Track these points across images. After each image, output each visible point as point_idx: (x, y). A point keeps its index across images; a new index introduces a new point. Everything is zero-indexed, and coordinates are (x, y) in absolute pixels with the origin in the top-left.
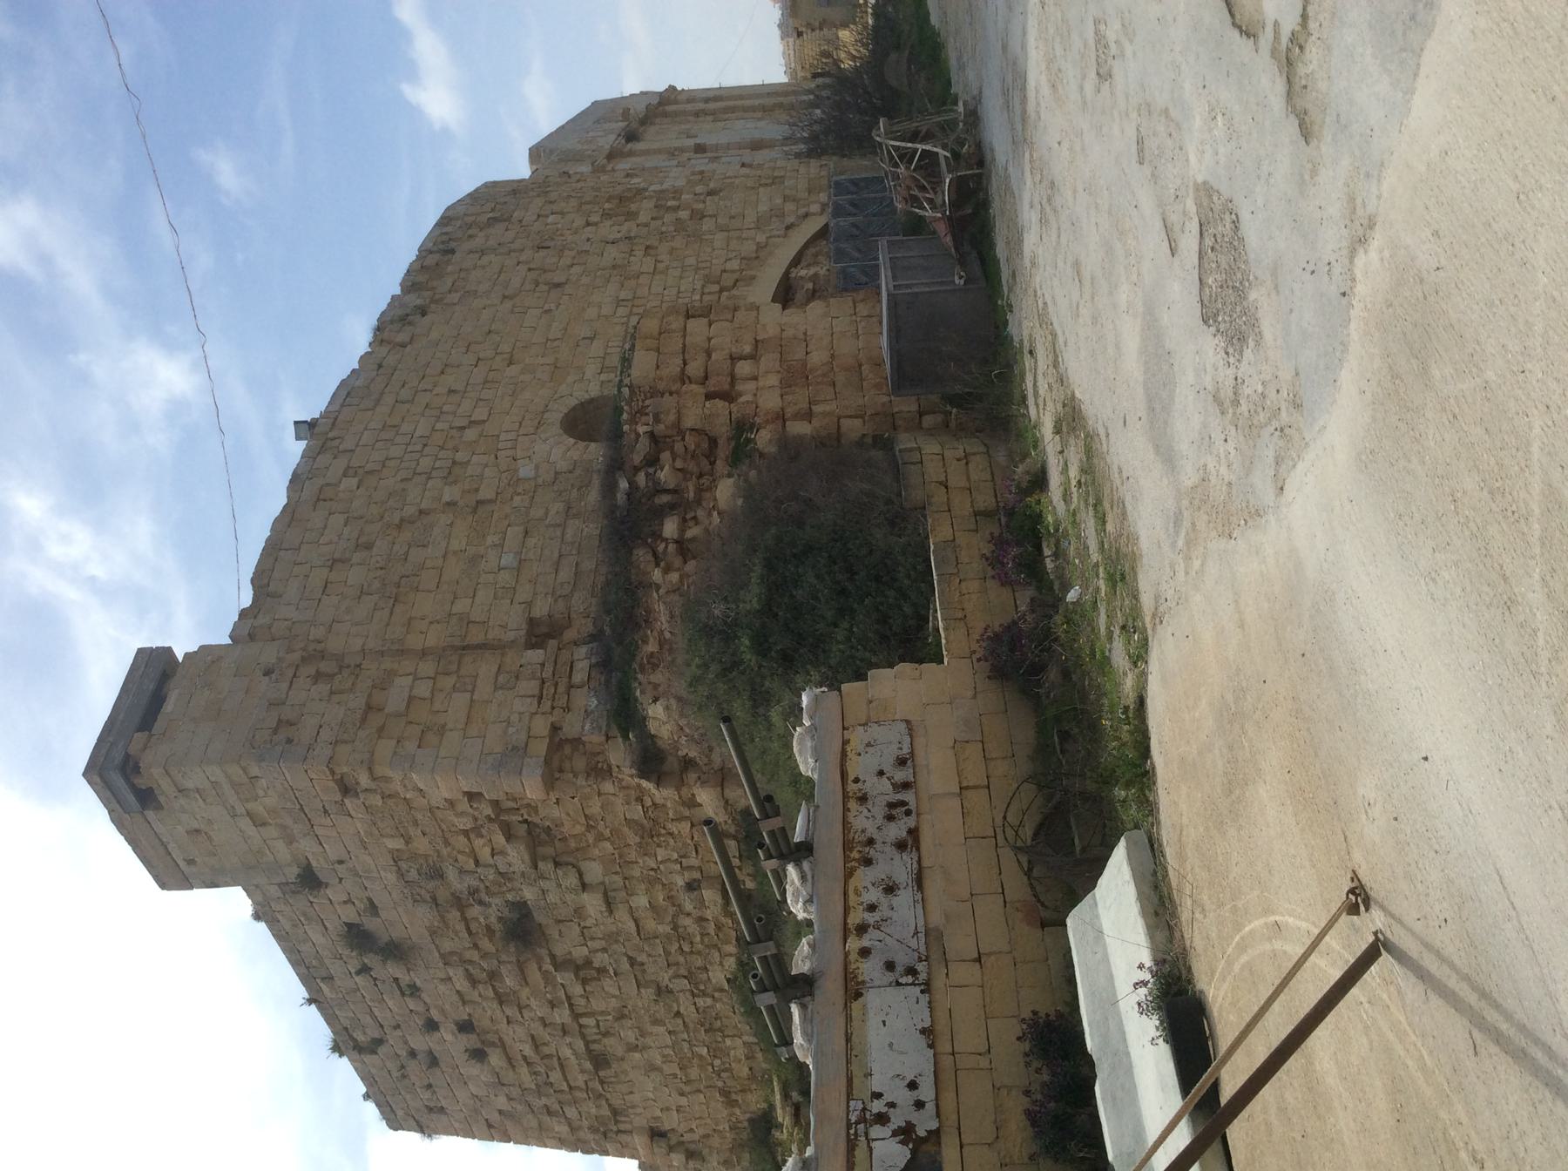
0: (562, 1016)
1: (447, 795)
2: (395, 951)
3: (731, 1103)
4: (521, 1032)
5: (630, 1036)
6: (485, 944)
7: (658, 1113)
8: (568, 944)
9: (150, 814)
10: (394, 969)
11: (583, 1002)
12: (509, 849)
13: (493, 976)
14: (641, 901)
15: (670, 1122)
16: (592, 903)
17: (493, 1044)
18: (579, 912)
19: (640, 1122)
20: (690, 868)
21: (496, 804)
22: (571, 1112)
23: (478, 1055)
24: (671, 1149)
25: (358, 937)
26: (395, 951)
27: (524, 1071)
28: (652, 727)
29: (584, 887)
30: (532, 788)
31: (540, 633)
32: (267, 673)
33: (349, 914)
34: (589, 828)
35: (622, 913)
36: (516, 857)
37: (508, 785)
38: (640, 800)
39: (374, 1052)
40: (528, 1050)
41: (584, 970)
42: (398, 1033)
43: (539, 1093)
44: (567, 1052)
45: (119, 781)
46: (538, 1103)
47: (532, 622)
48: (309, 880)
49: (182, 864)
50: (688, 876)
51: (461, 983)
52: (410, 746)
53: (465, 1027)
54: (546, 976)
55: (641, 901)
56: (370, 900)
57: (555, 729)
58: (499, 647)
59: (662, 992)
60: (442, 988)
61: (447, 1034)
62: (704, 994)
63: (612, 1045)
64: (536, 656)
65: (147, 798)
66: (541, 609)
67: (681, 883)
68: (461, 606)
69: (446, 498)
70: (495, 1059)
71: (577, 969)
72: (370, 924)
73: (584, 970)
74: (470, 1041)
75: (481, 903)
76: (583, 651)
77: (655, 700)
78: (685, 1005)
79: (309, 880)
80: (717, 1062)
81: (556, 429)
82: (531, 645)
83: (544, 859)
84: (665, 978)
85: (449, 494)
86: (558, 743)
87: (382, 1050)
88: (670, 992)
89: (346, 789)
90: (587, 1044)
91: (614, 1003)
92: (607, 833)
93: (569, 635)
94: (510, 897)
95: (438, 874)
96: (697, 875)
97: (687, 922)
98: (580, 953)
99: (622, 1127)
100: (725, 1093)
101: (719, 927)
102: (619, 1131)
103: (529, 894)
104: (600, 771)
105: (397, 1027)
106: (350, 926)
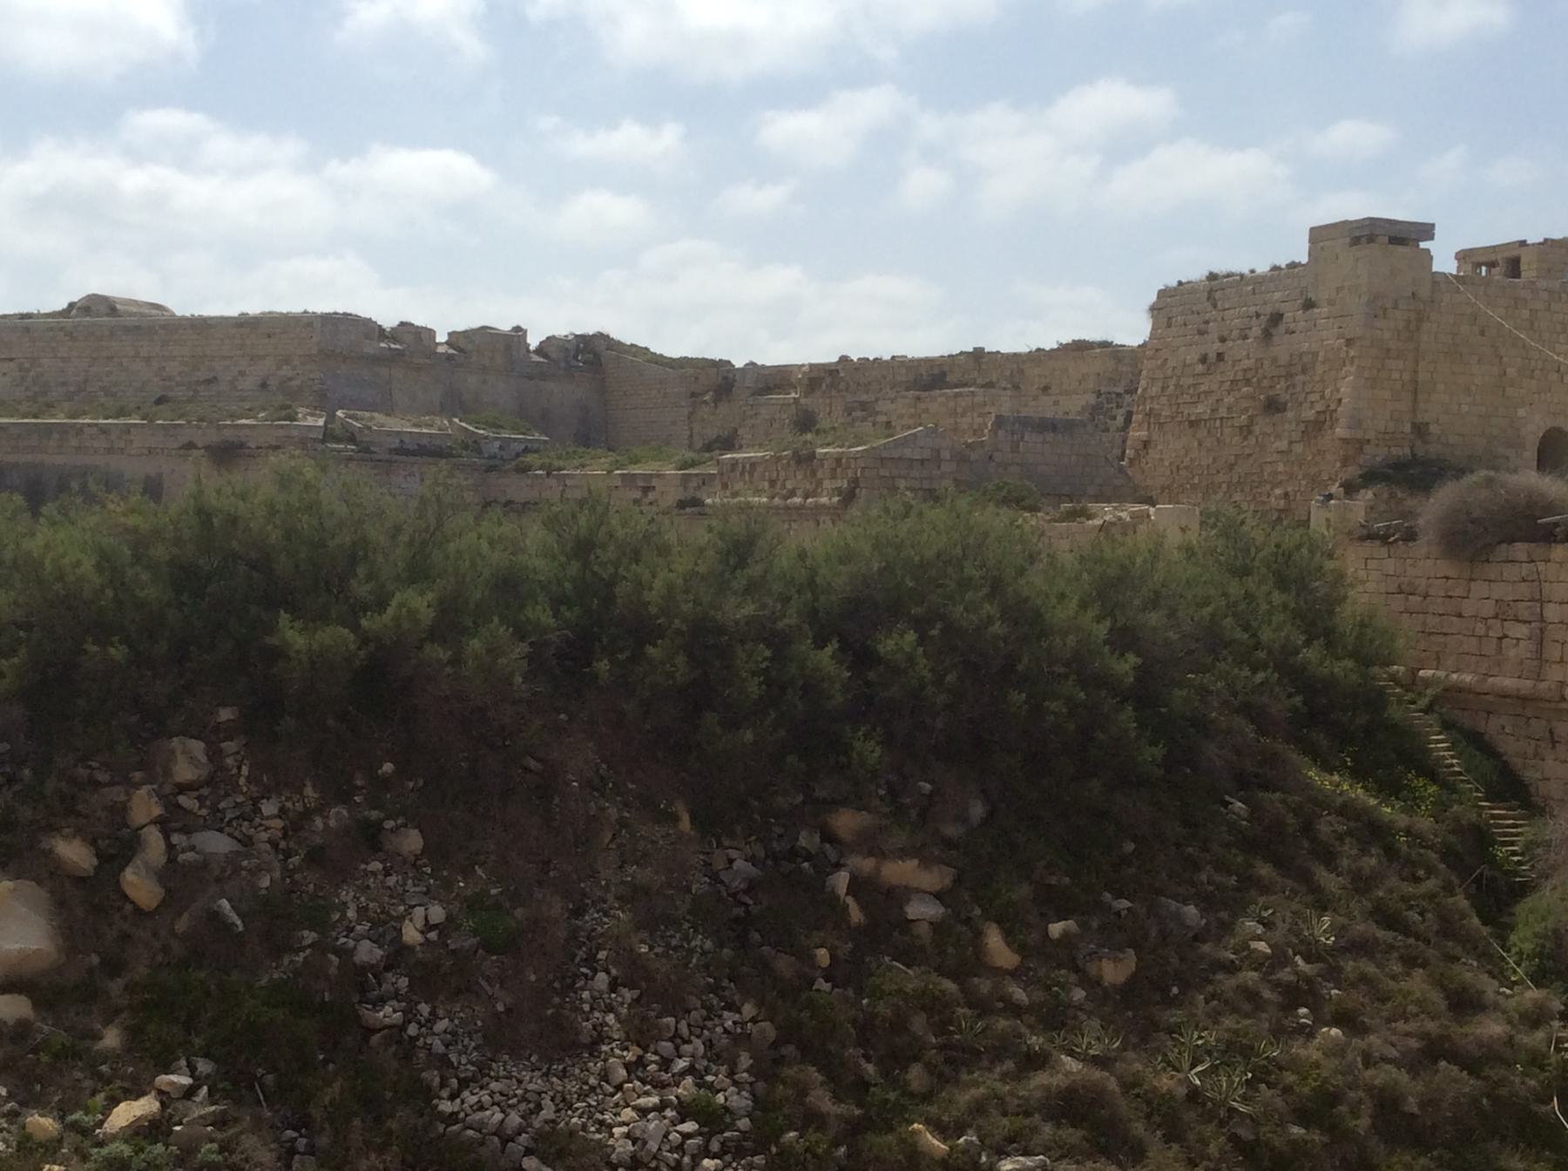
0: (1223, 412)
1: (1342, 390)
2: (1267, 335)
3: (1163, 489)
4: (1215, 387)
5: (1208, 443)
6: (1266, 383)
7: (1159, 447)
8: (1262, 425)
9: (1348, 240)
10: (1256, 331)
11: (1229, 423)
12: (1313, 411)
13: (1248, 382)
14: (1281, 468)
15: (1153, 454)
16: (1283, 445)
17: (1209, 369)
18: (1279, 437)
19: (1155, 437)
20: (1295, 495)
21: (1335, 410)
22: (1164, 400)
23: (1203, 359)
24: (1137, 451)
25: (1277, 318)
26: (1267, 335)
27: (1191, 381)
28: (1362, 491)
29: (1291, 443)
30: (1340, 431)
31: (1420, 430)
32: (1413, 294)
33: (1288, 316)
34: (1319, 451)
35: (1275, 457)
36: (1309, 414)
37: (1343, 421)
38: (1330, 479)
39: (1208, 299)
40: (1203, 388)
41: (1246, 430)
42: (1219, 319)
43: (1176, 386)
44: (1200, 409)
45: (1366, 232)
46: (1172, 382)
47: (1427, 424)
48: (1309, 305)
49: (1321, 244)
50: (1291, 494)
51: (1247, 363)
52: (1366, 374)
53: (1220, 356)
54: (1246, 409)
55: (1281, 468)
56: (1294, 332)
57: (1369, 441)
58: (1414, 411)
59: (1231, 467)
60: (1245, 353)
61: (1217, 346)
62: (1228, 487)
63: (1202, 433)
64: (1407, 428)
65: (1356, 241)
66: (1433, 428)
67: (1289, 489)
68: (1440, 387)
69: (1508, 370)
70: (1200, 368)
71: (1248, 427)
72: (1282, 328)
73: (1246, 430)
74: (1212, 356)
75: (1288, 388)
76: (1407, 451)
77: (1375, 495)
78: (1221, 478)
79: (1309, 305)
80: (1188, 486)
81: (1550, 423)
82: (1414, 424)
83: (1306, 427)
84: (1238, 469)
85: (1511, 371)
86: (1361, 444)
87: (1208, 305)
88: (1231, 470)
89: (1349, 342)
90: (1205, 420)
91: (1228, 441)
92: (1316, 459)
93: (1418, 443)
94: (1289, 405)
95: (1304, 371)
96: (1291, 498)
97: (1268, 487)
98: (1257, 430)
99: (1152, 426)
100: (1169, 487)
101: (1264, 503)
102: (1149, 423)
103: (1290, 415)
104: (1345, 462)
105: (1223, 319)
106: (1282, 315)
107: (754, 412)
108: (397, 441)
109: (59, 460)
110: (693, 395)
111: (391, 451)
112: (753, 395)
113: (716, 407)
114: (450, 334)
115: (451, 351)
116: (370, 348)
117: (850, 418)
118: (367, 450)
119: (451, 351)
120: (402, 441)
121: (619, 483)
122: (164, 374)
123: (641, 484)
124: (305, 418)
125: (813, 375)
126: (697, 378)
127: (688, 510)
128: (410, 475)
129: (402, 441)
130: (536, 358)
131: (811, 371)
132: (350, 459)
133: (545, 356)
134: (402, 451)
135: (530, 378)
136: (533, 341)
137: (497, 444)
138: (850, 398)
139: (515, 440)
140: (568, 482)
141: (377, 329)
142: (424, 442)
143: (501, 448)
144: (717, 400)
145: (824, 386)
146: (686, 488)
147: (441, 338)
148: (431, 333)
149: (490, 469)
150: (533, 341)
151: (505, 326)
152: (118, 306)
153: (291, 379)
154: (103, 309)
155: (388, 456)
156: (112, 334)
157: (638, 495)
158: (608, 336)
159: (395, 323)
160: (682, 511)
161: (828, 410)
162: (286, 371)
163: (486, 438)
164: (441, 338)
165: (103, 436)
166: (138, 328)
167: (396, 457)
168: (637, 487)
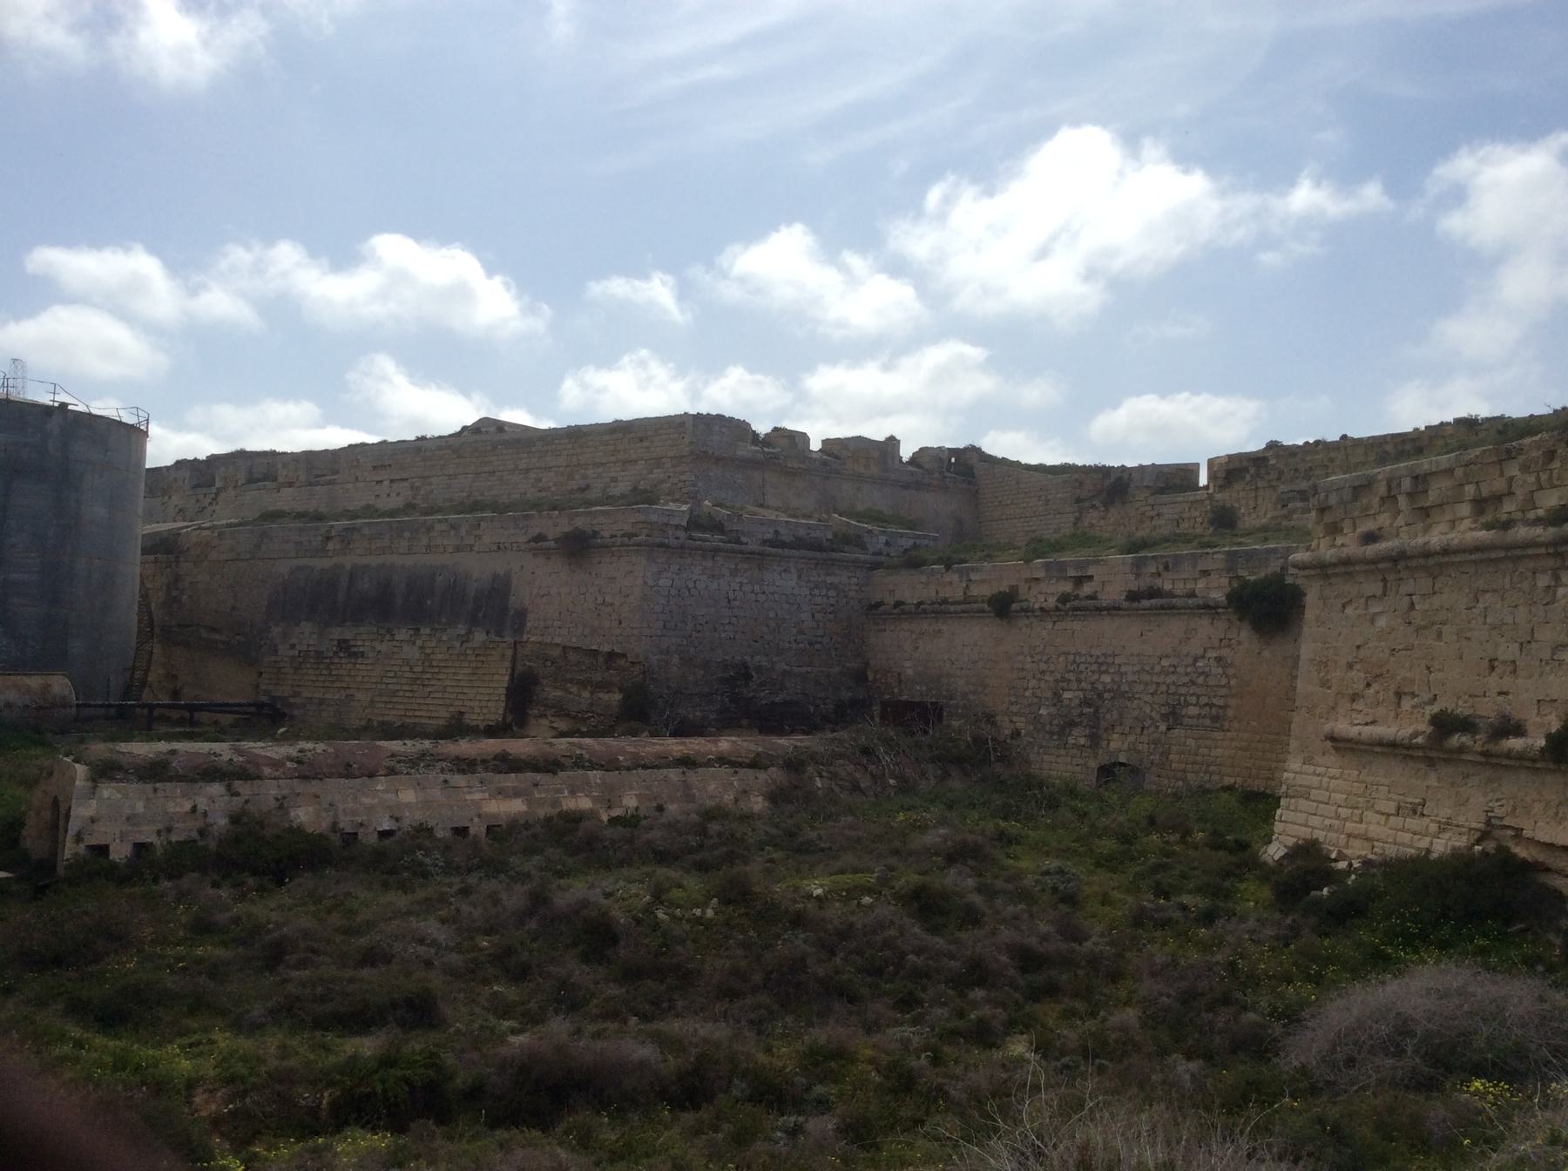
107: (1154, 513)
108: (771, 530)
109: (409, 561)
110: (1078, 500)
111: (764, 542)
112: (1152, 494)
113: (1107, 510)
114: (825, 442)
115: (825, 457)
116: (746, 450)
117: (1285, 511)
118: (738, 542)
119: (825, 457)
120: (777, 532)
121: (1040, 574)
122: (540, 485)
123: (1072, 573)
124: (667, 503)
125: (1231, 466)
126: (1081, 484)
127: (1146, 603)
128: (785, 571)
129: (777, 532)
130: (910, 468)
131: (1229, 461)
132: (717, 550)
133: (920, 466)
134: (776, 543)
135: (906, 487)
136: (906, 452)
137: (883, 539)
138: (1283, 488)
139: (901, 535)
140: (973, 576)
141: (750, 437)
142: (802, 532)
143: (887, 543)
144: (1108, 504)
145: (1248, 477)
146: (1138, 575)
147: (815, 446)
148: (804, 437)
149: (875, 566)
150: (906, 452)
151: (880, 436)
152: (506, 428)
153: (661, 482)
154: (492, 429)
155: (761, 548)
156: (494, 448)
157: (1067, 587)
158: (980, 449)
159: (768, 430)
160: (1135, 605)
161: (1252, 504)
162: (658, 474)
163: (870, 532)
164: (815, 446)
165: (452, 532)
166: (518, 441)
167: (769, 549)
168: (1066, 579)
